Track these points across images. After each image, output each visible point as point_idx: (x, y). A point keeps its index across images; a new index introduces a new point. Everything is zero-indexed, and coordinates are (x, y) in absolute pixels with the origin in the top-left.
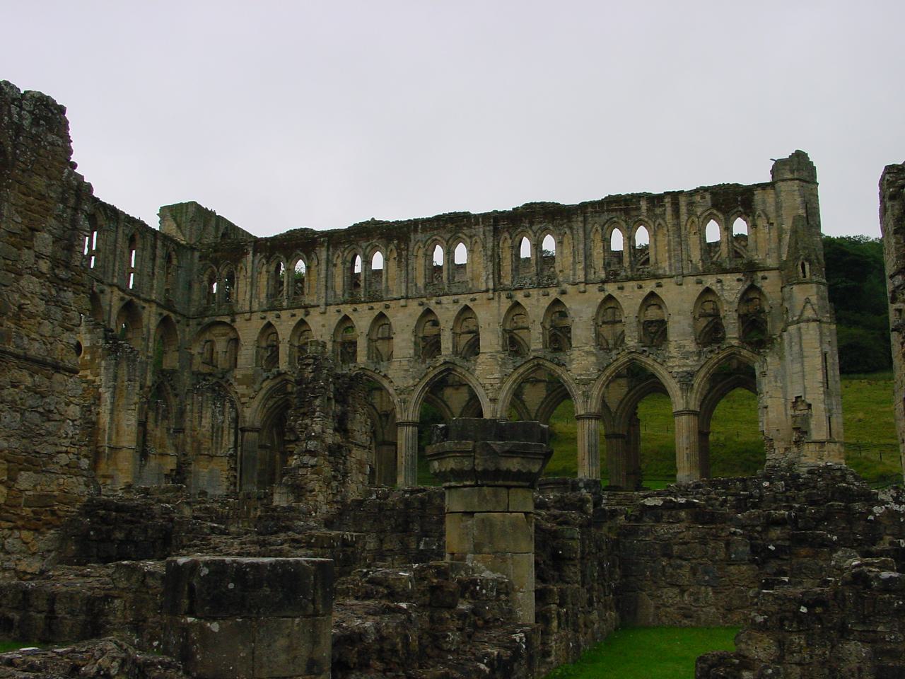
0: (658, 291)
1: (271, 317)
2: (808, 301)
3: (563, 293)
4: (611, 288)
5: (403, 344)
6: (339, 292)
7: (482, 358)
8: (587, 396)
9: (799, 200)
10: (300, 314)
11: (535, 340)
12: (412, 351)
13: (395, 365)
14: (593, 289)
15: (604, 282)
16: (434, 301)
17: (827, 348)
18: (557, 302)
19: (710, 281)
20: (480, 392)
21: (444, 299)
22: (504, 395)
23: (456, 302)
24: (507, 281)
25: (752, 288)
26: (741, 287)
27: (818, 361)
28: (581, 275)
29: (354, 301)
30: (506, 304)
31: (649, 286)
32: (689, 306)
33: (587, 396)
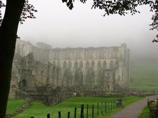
0: (106, 60)
1: (54, 60)
2: (121, 64)
3: (94, 60)
6: (64, 58)
7: (83, 68)
8: (96, 73)
9: (124, 50)
12: (74, 66)
15: (99, 59)
16: (77, 60)
17: (123, 70)
19: (112, 59)
20: (83, 72)
21: (78, 60)
22: (86, 73)
23: (80, 60)
26: (116, 61)
27: (121, 71)
32: (109, 62)
33: (96, 73)
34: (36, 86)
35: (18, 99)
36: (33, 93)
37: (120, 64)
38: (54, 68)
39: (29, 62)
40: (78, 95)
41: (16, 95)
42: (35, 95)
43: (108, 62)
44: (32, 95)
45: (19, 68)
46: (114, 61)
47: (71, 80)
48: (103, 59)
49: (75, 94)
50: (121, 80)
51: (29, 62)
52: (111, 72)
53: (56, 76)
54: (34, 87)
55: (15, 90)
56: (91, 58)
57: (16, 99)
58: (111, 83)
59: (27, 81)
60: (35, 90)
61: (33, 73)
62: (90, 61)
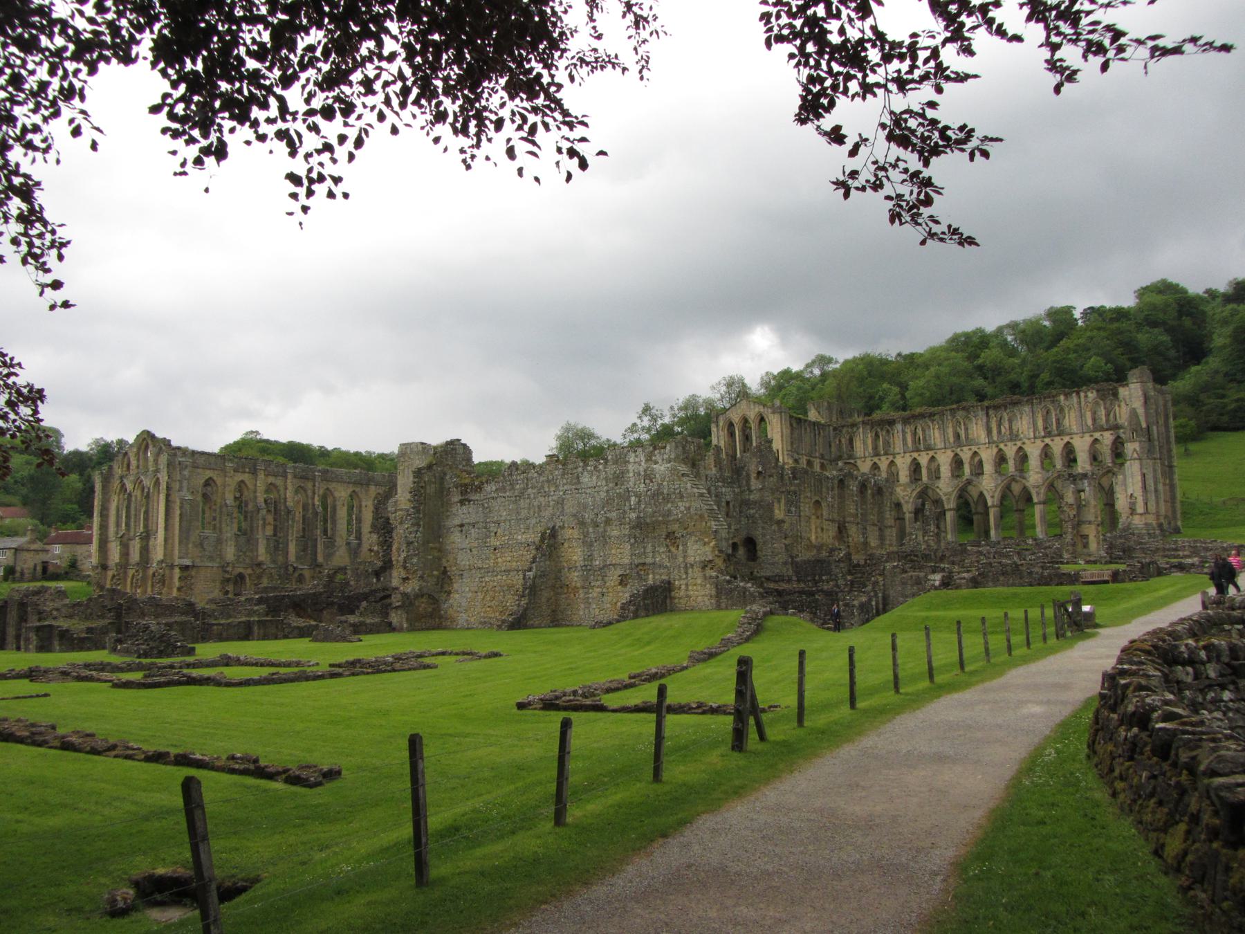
1: (876, 459)
4: (1047, 440)
5: (945, 471)
8: (1038, 494)
10: (891, 458)
11: (1011, 467)
13: (942, 481)
14: (1038, 441)
18: (1021, 448)
19: (1097, 435)
20: (985, 493)
22: (997, 495)
24: (995, 438)
25: (1119, 437)
28: (1032, 435)
29: (918, 450)
30: (995, 450)
31: (1066, 439)
34: (792, 557)
35: (727, 608)
36: (784, 586)
37: (1131, 448)
38: (863, 487)
39: (759, 473)
40: (946, 584)
41: (718, 595)
42: (790, 593)
43: (1081, 445)
44: (780, 593)
45: (728, 498)
46: (1107, 438)
47: (938, 527)
48: (1059, 435)
49: (937, 578)
50: (1140, 509)
51: (759, 473)
52: (1090, 484)
53: (873, 518)
54: (785, 563)
55: (711, 577)
56: (1014, 437)
57: (719, 607)
58: (1093, 527)
59: (759, 541)
60: (791, 572)
61: (779, 513)
62: (1010, 451)
